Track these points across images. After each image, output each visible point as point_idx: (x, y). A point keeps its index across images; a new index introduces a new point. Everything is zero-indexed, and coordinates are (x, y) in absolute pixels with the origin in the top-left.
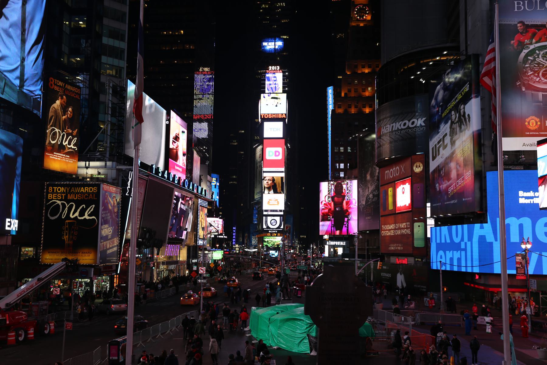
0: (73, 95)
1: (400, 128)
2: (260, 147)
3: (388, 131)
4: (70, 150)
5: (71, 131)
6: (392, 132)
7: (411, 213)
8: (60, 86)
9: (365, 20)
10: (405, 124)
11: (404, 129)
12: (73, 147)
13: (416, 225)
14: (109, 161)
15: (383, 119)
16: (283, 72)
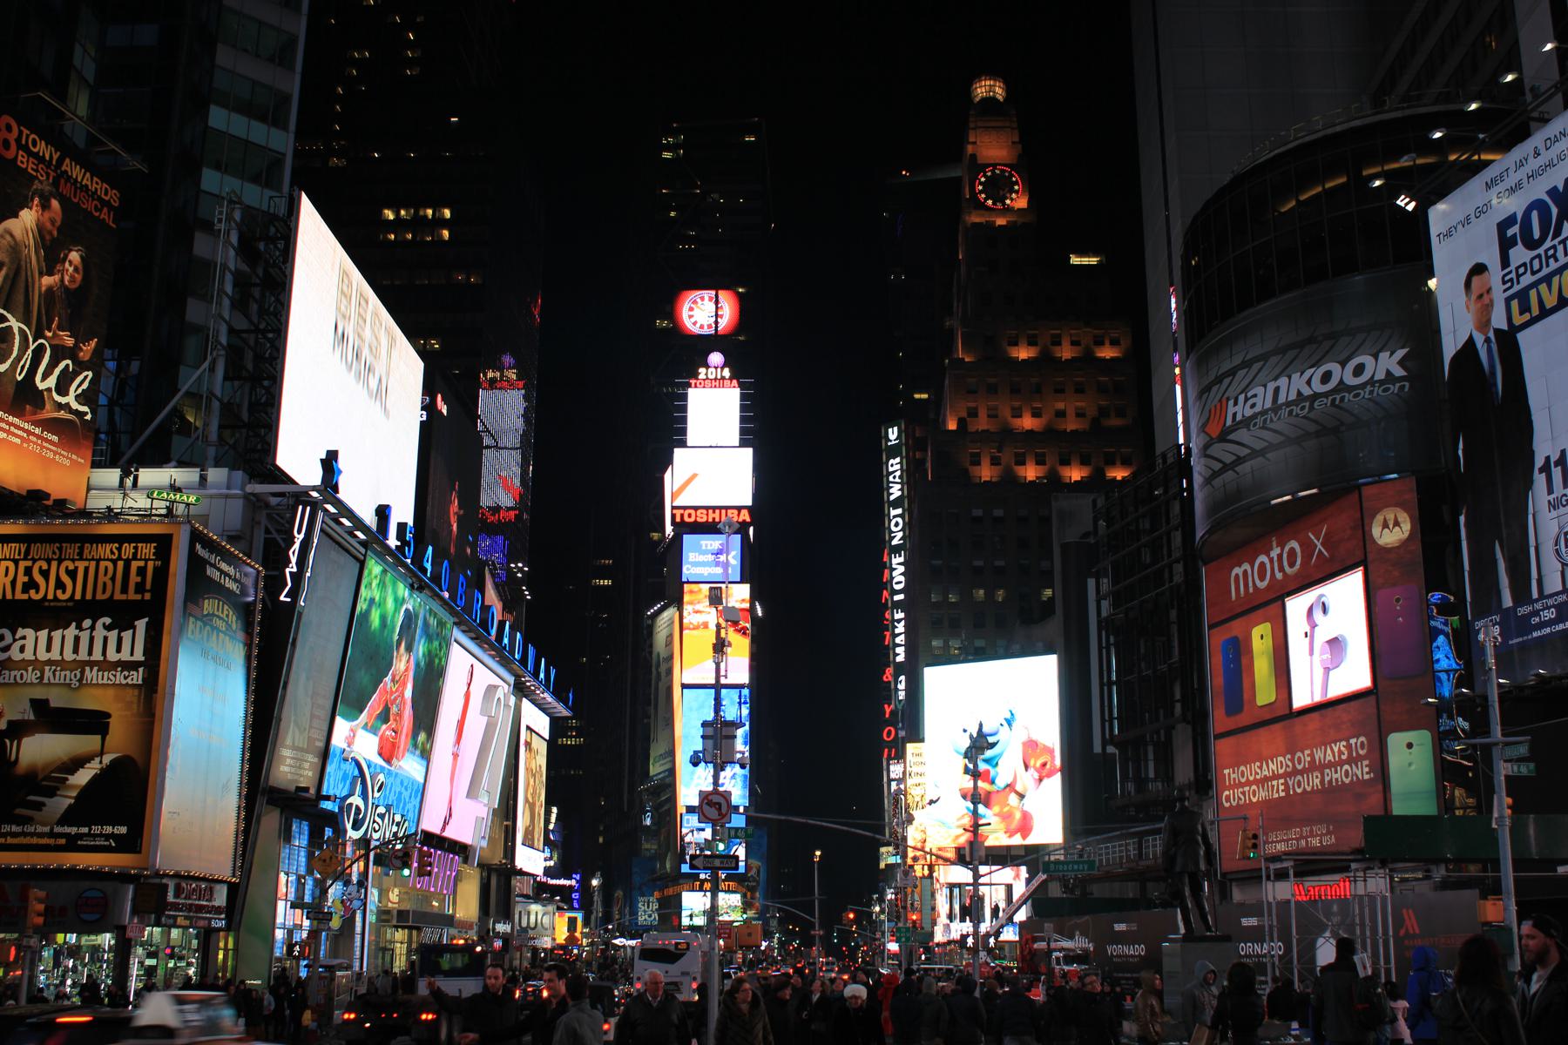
0: (89, 206)
1: (1307, 392)
2: (671, 612)
3: (1258, 409)
4: (62, 414)
5: (70, 342)
6: (1276, 408)
7: (1372, 699)
8: (40, 159)
9: (1008, 210)
10: (1326, 378)
11: (1326, 395)
12: (75, 406)
13: (1396, 741)
14: (218, 464)
15: (1232, 373)
16: (741, 386)
